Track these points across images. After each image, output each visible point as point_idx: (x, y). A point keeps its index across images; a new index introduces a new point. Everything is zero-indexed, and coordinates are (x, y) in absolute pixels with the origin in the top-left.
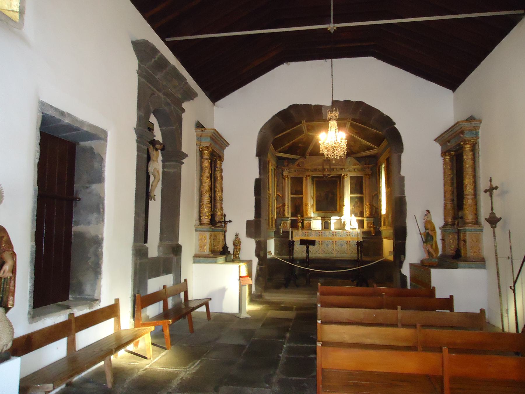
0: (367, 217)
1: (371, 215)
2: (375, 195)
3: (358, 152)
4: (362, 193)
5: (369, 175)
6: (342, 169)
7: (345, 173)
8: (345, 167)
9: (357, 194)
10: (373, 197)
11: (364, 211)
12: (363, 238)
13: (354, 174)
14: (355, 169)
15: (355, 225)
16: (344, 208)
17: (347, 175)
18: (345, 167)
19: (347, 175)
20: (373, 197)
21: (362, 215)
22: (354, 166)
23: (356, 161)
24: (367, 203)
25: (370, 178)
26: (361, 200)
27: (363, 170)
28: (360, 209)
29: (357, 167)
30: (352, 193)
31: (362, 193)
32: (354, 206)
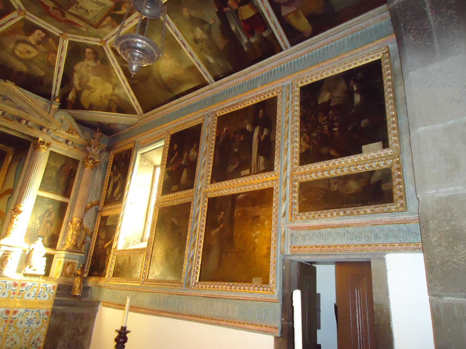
0: (68, 250)
1: (75, 248)
2: (92, 206)
3: (91, 107)
4: (66, 194)
5: (94, 163)
6: (41, 128)
7: (48, 139)
8: (52, 127)
9: (56, 193)
10: (86, 209)
11: (61, 235)
12: (56, 303)
13: (61, 149)
14: (67, 142)
15: (39, 264)
16: (19, 216)
17: (48, 145)
18: (52, 127)
19: (48, 145)
20: (86, 209)
21: (52, 242)
22: (68, 131)
23: (75, 126)
24: (75, 220)
25: (92, 169)
26: (62, 207)
27: (85, 148)
28: (53, 230)
29: (76, 137)
30: (43, 187)
31: (66, 194)
32: (41, 219)
